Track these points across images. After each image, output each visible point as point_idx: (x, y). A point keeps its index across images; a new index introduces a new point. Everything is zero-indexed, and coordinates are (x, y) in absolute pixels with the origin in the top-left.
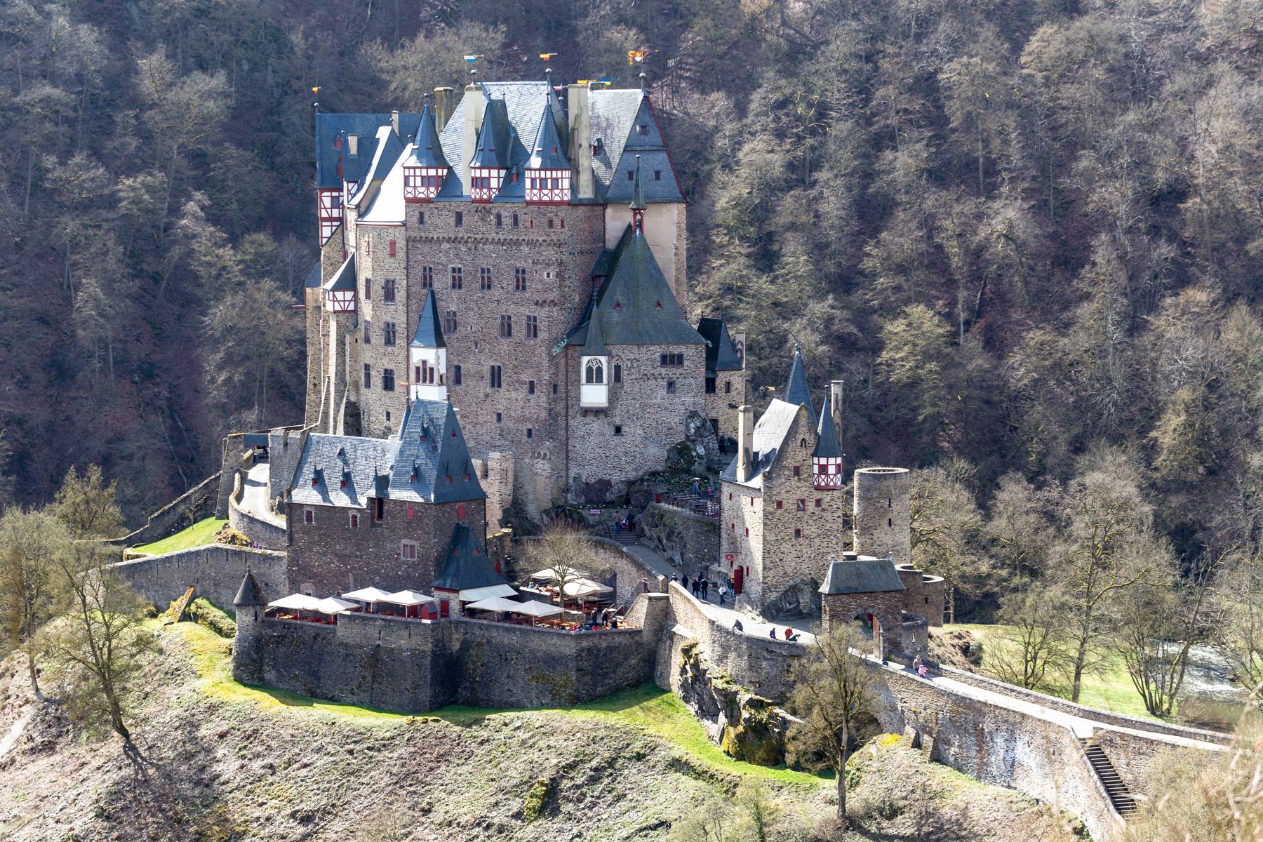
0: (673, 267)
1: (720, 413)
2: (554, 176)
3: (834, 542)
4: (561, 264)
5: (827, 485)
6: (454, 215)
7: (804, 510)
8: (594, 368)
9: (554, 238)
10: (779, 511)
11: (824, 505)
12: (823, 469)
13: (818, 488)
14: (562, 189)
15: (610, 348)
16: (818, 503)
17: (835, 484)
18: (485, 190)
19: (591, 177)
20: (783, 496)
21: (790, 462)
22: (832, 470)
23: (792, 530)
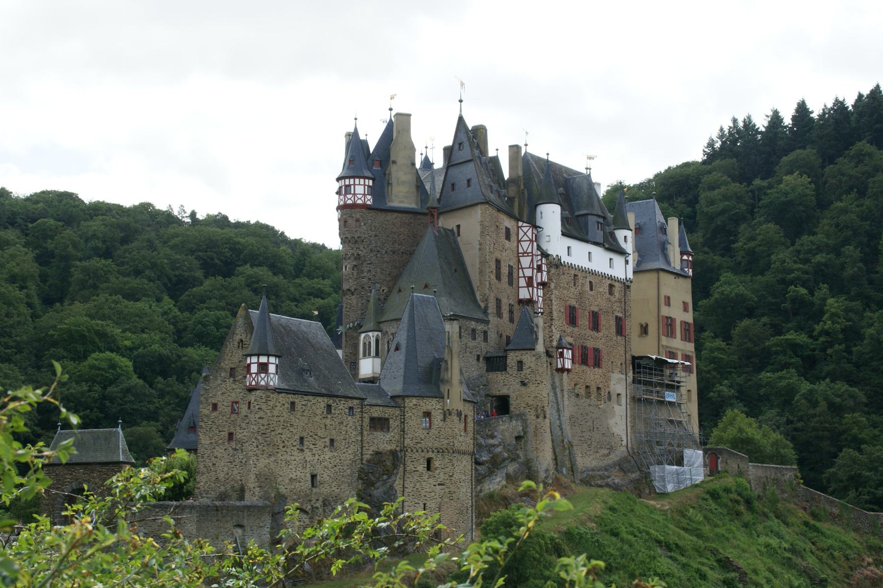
0: (478, 261)
1: (511, 390)
2: (347, 183)
3: (255, 444)
5: (250, 384)
8: (367, 343)
10: (215, 414)
12: (249, 366)
13: (251, 390)
14: (355, 194)
15: (382, 326)
17: (257, 383)
19: (414, 189)
20: (219, 399)
22: (254, 369)
23: (225, 434)
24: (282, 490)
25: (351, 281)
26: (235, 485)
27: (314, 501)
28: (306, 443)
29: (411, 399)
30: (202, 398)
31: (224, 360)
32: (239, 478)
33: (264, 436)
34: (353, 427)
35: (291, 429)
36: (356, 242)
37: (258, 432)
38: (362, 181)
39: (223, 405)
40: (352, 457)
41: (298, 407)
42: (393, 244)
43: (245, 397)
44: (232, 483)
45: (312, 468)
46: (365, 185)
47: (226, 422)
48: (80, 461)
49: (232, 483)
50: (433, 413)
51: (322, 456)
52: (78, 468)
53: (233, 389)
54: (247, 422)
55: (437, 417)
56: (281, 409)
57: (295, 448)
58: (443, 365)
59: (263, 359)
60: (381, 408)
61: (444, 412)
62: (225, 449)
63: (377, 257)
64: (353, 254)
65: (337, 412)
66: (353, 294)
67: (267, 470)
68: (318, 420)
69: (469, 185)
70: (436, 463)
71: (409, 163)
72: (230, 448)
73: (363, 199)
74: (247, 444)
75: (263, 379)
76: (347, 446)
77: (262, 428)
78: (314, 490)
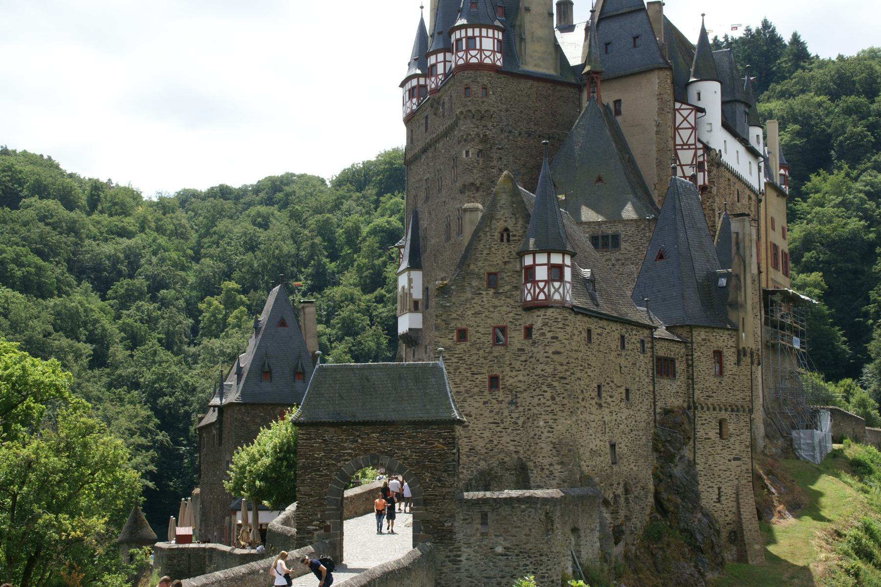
2: (470, 32)
3: (548, 395)
4: (485, 139)
5: (535, 298)
6: (423, 121)
7: (505, 345)
9: (473, 109)
10: (463, 346)
11: (535, 335)
12: (530, 271)
14: (481, 50)
16: (528, 331)
17: (548, 297)
18: (433, 79)
19: (551, 49)
20: (469, 322)
21: (481, 266)
22: (541, 273)
23: (484, 378)
24: (586, 470)
25: (475, 171)
26: (506, 459)
27: (615, 485)
28: (604, 394)
29: (699, 329)
30: (439, 320)
31: (476, 260)
32: (512, 448)
33: (563, 381)
34: (646, 371)
35: (589, 371)
36: (482, 117)
37: (554, 376)
38: (490, 32)
39: (477, 332)
40: (646, 417)
41: (594, 337)
42: (528, 123)
43: (517, 320)
44: (501, 456)
45: (610, 434)
46: (494, 38)
47: (485, 358)
48: (374, 419)
49: (501, 456)
50: (725, 353)
51: (619, 415)
52: (367, 429)
53: (495, 307)
54: (523, 358)
55: (730, 358)
56: (579, 340)
57: (593, 402)
58: (733, 281)
59: (556, 259)
60: (666, 343)
61: (738, 351)
62: (485, 403)
63: (508, 141)
64: (478, 135)
65: (630, 348)
66: (478, 189)
67: (568, 435)
68: (614, 360)
69: (635, 46)
70: (731, 427)
71: (546, 12)
72: (494, 401)
73: (492, 57)
74: (525, 395)
75: (557, 290)
76: (641, 401)
77: (560, 368)
78: (615, 468)
